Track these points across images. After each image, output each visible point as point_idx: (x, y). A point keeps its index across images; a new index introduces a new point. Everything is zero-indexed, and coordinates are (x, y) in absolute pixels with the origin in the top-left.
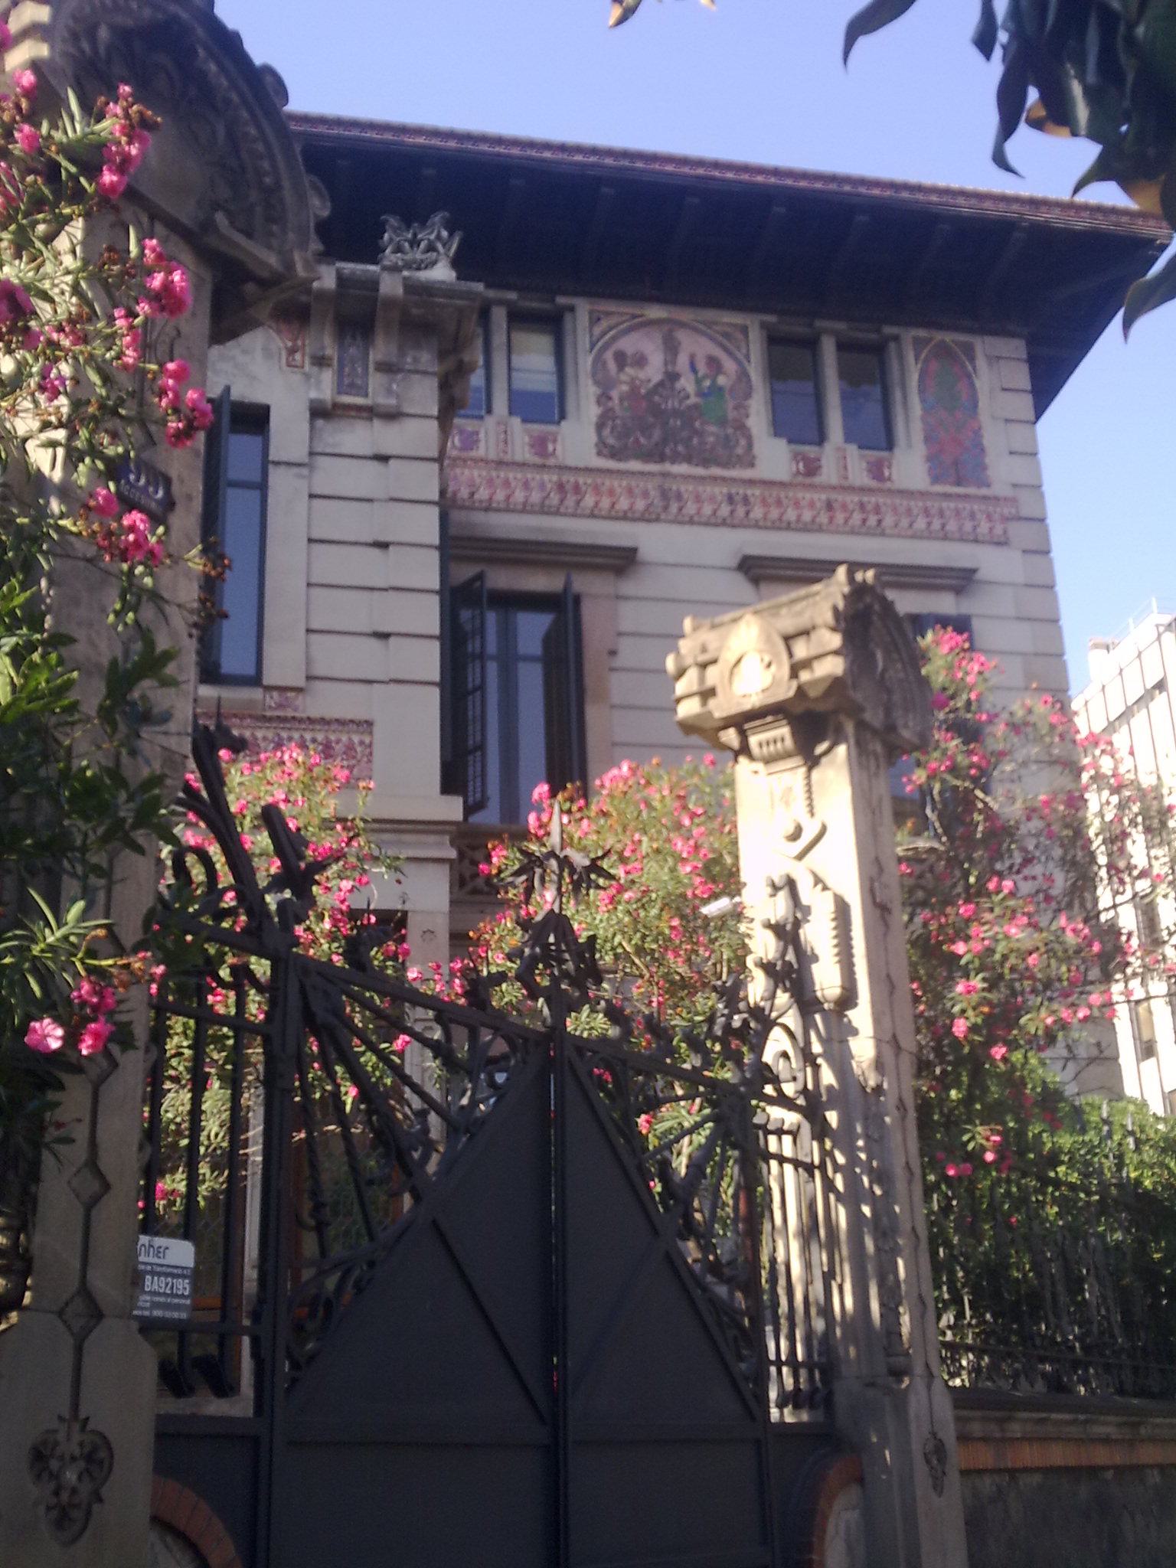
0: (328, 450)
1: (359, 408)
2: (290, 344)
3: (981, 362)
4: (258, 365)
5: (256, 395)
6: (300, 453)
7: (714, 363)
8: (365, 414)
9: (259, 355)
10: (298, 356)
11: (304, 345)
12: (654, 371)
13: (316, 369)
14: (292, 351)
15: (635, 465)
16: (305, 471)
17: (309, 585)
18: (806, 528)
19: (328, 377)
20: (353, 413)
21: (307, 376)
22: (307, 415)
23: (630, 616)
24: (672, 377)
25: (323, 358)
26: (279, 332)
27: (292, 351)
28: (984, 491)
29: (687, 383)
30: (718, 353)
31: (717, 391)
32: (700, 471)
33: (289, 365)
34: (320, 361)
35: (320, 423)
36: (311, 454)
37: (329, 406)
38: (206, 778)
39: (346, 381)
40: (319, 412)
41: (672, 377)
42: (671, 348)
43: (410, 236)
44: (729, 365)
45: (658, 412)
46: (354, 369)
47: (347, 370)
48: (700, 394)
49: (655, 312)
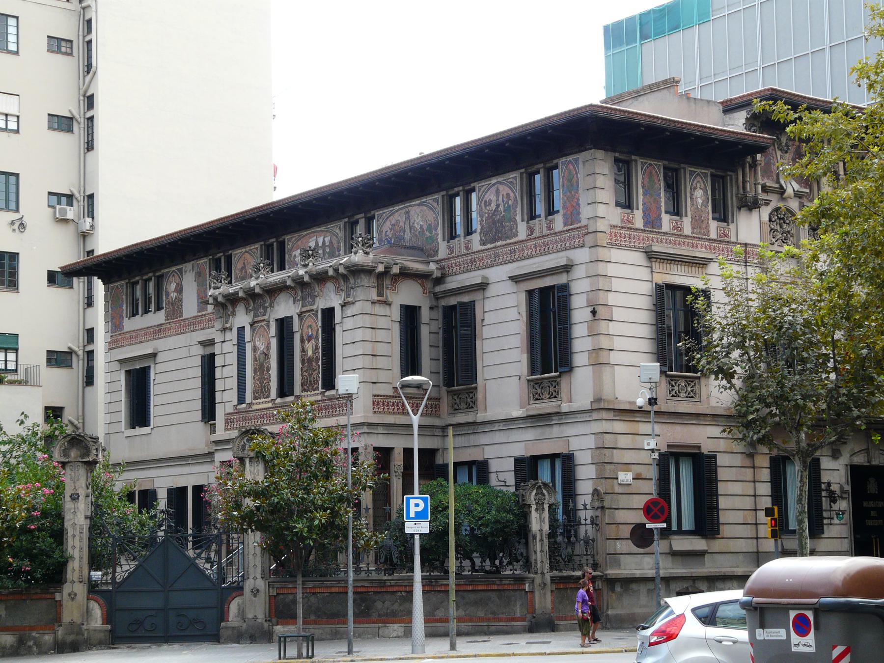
3: (581, 165)
4: (333, 295)
7: (508, 195)
12: (493, 206)
15: (489, 246)
18: (529, 257)
23: (489, 305)
24: (498, 206)
28: (579, 225)
29: (501, 208)
30: (510, 192)
31: (509, 206)
32: (504, 243)
41: (498, 206)
42: (498, 192)
44: (512, 195)
45: (494, 223)
48: (505, 211)
49: (494, 181)
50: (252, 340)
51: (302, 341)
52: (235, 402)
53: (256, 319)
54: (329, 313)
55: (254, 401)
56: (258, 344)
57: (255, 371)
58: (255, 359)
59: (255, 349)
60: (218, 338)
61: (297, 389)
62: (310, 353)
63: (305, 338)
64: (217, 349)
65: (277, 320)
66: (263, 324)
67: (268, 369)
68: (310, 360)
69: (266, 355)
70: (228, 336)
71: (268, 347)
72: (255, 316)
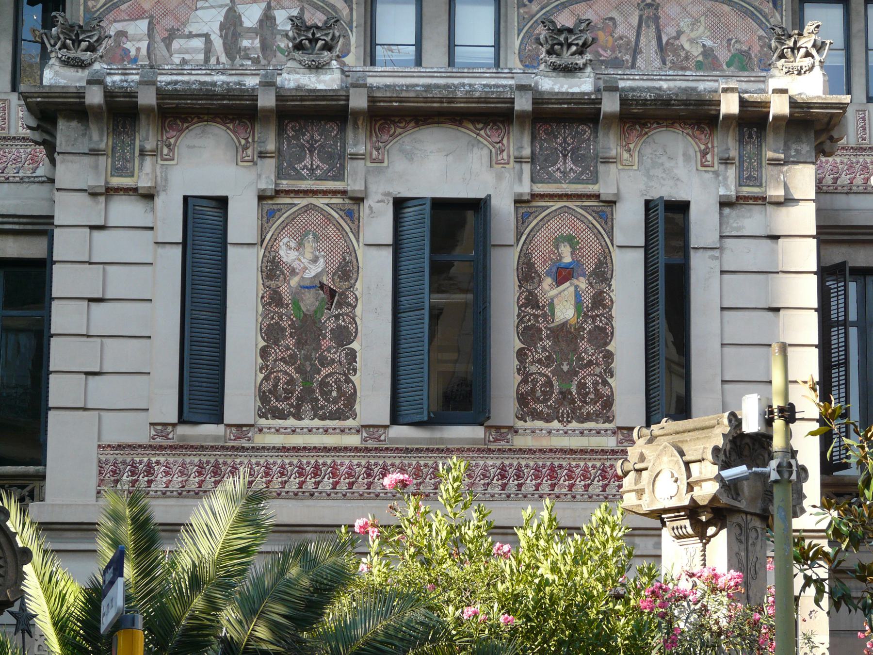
0: (734, 233)
1: (756, 198)
2: (703, 147)
4: (681, 169)
5: (679, 194)
6: (712, 239)
8: (760, 202)
9: (681, 159)
10: (709, 157)
11: (713, 147)
13: (722, 167)
14: (704, 154)
16: (717, 253)
17: (722, 345)
19: (731, 173)
20: (751, 202)
21: (716, 174)
22: (718, 205)
25: (728, 159)
26: (694, 137)
27: (704, 154)
33: (703, 165)
34: (726, 161)
35: (727, 211)
36: (722, 237)
37: (734, 200)
38: (550, 311)
39: (746, 174)
40: (725, 204)
43: (791, 44)
46: (750, 163)
47: (746, 164)
50: (263, 239)
51: (527, 273)
52: (167, 408)
53: (285, 184)
54: (669, 220)
55: (263, 422)
56: (288, 255)
57: (272, 333)
58: (274, 299)
59: (272, 269)
60: (69, 211)
61: (504, 406)
62: (565, 312)
63: (541, 268)
64: (66, 245)
65: (400, 204)
66: (320, 202)
67: (344, 336)
68: (565, 335)
69: (335, 293)
70: (125, 211)
71: (347, 271)
72: (280, 174)
